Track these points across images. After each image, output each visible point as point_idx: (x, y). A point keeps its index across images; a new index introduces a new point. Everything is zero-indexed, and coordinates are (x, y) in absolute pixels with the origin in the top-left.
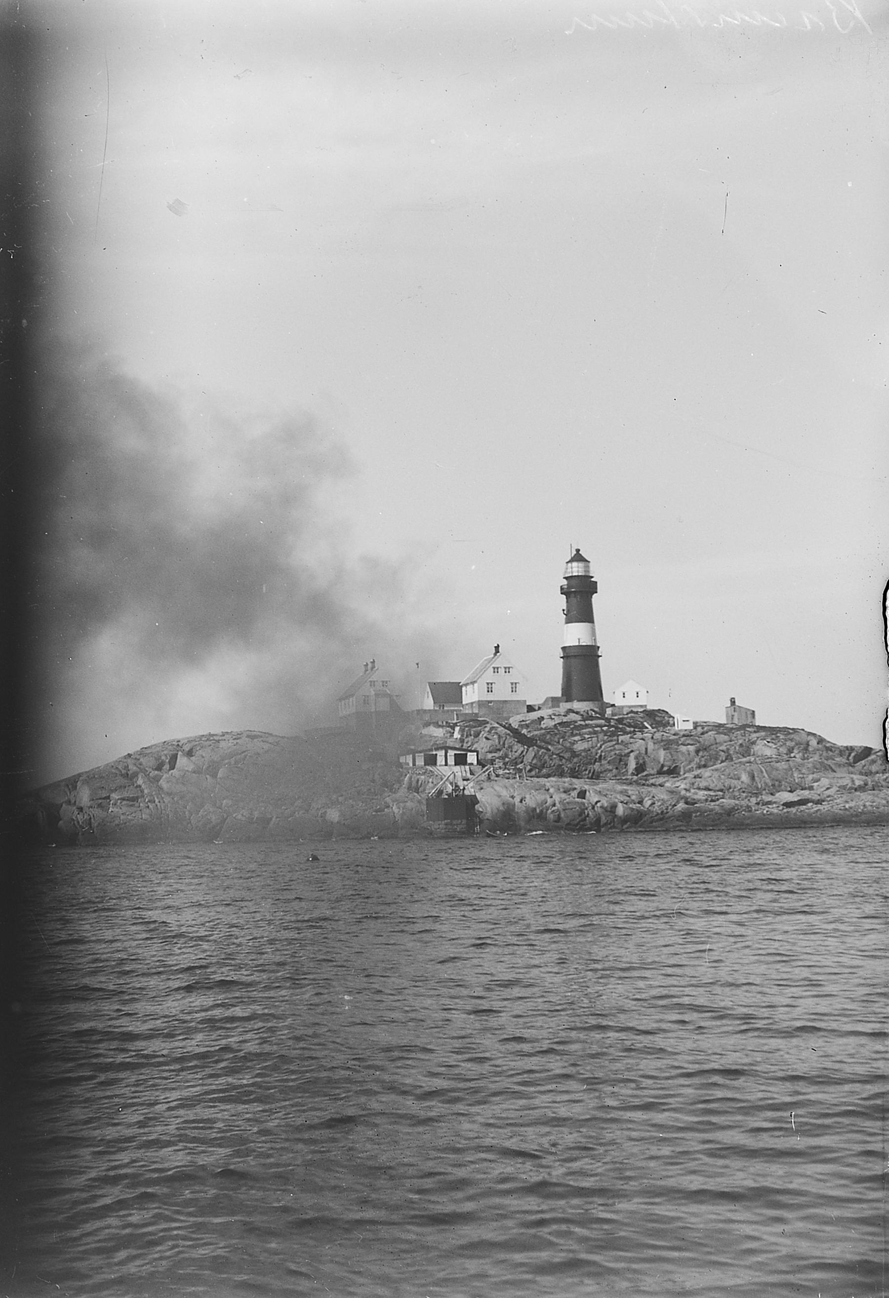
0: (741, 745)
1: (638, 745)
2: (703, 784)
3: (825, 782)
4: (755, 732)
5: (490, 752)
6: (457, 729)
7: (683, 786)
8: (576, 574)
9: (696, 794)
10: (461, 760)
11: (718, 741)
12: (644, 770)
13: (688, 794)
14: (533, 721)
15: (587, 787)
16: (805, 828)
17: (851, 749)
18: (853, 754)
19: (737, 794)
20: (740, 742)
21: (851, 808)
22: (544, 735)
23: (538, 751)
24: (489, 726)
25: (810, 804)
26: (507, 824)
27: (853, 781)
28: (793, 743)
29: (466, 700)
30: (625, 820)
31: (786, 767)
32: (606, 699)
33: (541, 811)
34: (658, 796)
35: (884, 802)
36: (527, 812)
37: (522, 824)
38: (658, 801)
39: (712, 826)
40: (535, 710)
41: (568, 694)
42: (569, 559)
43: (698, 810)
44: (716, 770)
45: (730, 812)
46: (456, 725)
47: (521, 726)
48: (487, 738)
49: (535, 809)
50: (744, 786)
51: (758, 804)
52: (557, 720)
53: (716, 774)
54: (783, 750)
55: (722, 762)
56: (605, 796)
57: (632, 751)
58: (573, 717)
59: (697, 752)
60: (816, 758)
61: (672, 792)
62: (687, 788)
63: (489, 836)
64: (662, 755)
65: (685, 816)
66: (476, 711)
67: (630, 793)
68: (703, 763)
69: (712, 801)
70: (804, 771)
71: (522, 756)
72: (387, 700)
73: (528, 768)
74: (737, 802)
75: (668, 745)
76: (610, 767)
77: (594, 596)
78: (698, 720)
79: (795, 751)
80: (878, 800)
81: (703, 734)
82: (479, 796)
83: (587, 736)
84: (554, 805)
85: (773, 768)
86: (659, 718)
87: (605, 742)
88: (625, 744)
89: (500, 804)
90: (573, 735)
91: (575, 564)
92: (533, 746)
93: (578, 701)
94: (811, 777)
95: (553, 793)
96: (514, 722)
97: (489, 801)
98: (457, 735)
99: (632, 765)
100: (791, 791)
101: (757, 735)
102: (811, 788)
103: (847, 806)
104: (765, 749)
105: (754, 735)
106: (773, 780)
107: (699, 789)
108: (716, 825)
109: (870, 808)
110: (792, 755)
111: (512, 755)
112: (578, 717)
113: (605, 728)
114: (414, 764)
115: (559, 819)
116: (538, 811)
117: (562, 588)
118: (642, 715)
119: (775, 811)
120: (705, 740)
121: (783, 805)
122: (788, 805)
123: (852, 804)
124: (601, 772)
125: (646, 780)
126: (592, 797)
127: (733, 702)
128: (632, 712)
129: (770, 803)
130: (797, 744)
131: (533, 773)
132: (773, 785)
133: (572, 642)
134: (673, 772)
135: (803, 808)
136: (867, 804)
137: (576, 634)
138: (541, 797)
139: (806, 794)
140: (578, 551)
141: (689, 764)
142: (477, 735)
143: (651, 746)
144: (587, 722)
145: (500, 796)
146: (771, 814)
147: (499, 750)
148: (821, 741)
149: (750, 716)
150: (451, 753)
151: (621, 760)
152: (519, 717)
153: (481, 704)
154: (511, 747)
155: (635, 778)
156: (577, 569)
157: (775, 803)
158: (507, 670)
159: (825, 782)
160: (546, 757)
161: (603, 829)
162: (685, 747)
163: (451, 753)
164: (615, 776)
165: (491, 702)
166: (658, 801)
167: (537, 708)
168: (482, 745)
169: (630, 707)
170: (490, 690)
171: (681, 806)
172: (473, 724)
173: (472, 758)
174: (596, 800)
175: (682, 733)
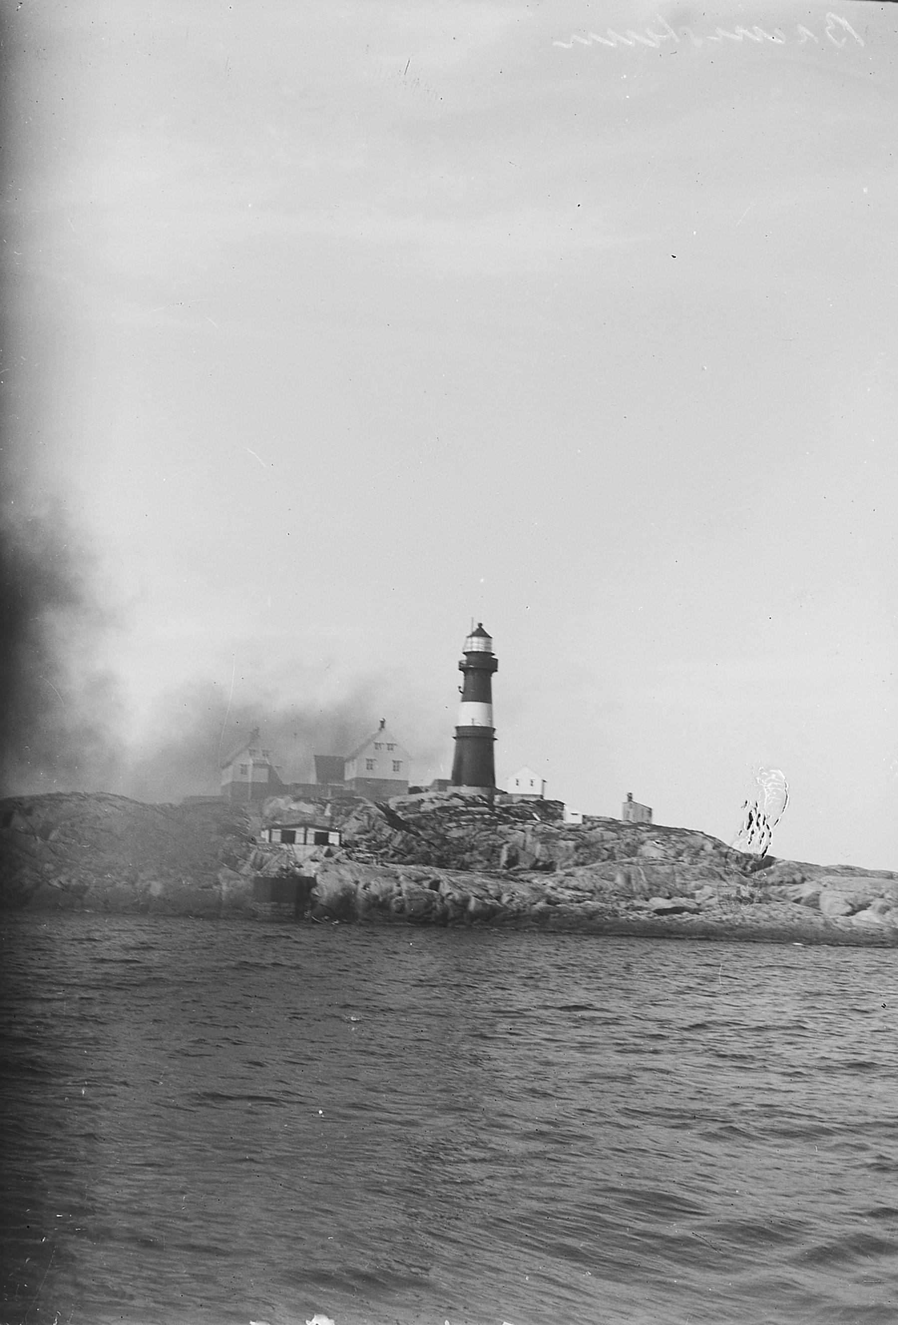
0: (628, 844)
1: (517, 836)
2: (573, 882)
3: (708, 890)
4: (648, 831)
5: (359, 833)
6: (329, 805)
7: (550, 884)
8: (475, 650)
9: (562, 893)
10: (321, 840)
11: (605, 838)
12: (516, 864)
13: (553, 893)
14: (412, 804)
15: (442, 877)
16: (669, 938)
17: (749, 857)
18: (751, 863)
19: (606, 896)
20: (628, 840)
21: (727, 920)
22: (419, 818)
23: (407, 835)
24: (362, 805)
25: (685, 913)
26: (344, 909)
27: (739, 892)
28: (684, 846)
29: (347, 777)
30: (475, 916)
31: (668, 871)
32: (499, 786)
33: (385, 900)
34: (518, 893)
35: (766, 916)
36: (367, 900)
37: (360, 912)
38: (518, 897)
39: (569, 929)
40: (422, 792)
41: (457, 779)
42: (470, 633)
43: (559, 911)
44: (591, 869)
45: (592, 915)
46: (329, 802)
47: (399, 808)
48: (357, 819)
49: (377, 897)
50: (616, 888)
51: (627, 908)
52: (438, 804)
53: (589, 873)
54: (671, 852)
55: (604, 860)
56: (460, 888)
57: (507, 842)
58: (456, 802)
59: (577, 848)
60: (706, 863)
61: (535, 889)
62: (554, 885)
63: (314, 922)
64: (538, 849)
65: (543, 916)
66: (353, 788)
67: (489, 886)
68: (581, 860)
69: (579, 902)
70: (688, 877)
71: (389, 840)
72: (265, 771)
73: (391, 852)
74: (603, 905)
75: (546, 838)
76: (480, 858)
77: (494, 674)
78: (588, 814)
79: (685, 855)
80: (759, 914)
81: (591, 829)
82: (319, 878)
83: (463, 823)
84: (400, 894)
85: (653, 871)
86: (550, 809)
87: (481, 830)
88: (502, 835)
89: (339, 888)
90: (450, 821)
91: (475, 639)
92: (414, 832)
93: (469, 785)
94: (693, 883)
95: (402, 881)
96: (392, 804)
97: (328, 885)
98: (328, 813)
99: (504, 857)
100: (668, 898)
101: (649, 834)
102: (692, 896)
103: (724, 917)
104: (652, 850)
105: (645, 835)
106: (651, 884)
107: (567, 888)
108: (572, 928)
109: (748, 922)
110: (680, 858)
111: (380, 838)
112: (461, 802)
113: (487, 816)
114: (270, 841)
115: (402, 909)
116: (380, 899)
117: (460, 663)
118: (532, 805)
119: (643, 917)
120: (590, 836)
121: (655, 912)
122: (661, 912)
123: (730, 916)
124: (471, 863)
125: (517, 875)
126: (445, 889)
127: (630, 798)
128: (523, 801)
129: (641, 908)
130: (688, 847)
131: (396, 859)
132: (650, 890)
133: (465, 721)
134: (548, 868)
135: (676, 916)
136: (746, 917)
137: (471, 714)
138: (385, 884)
139: (682, 901)
140: (480, 625)
141: (566, 860)
142: (348, 814)
143: (529, 838)
144: (469, 808)
145: (341, 880)
146: (638, 920)
147: (368, 832)
148: (718, 845)
149: (646, 814)
150: (312, 831)
151: (493, 851)
152: (398, 799)
153: (359, 781)
154: (380, 830)
155: (505, 871)
156: (477, 645)
157: (646, 909)
158: (391, 746)
159: (708, 890)
160: (414, 843)
161: (450, 925)
162: (564, 842)
163: (312, 831)
164: (485, 868)
165: (369, 780)
166: (518, 897)
167: (423, 790)
168: (352, 826)
169: (523, 795)
170: (370, 767)
171: (541, 904)
172: (346, 803)
173: (334, 838)
174: (448, 891)
175: (566, 827)
